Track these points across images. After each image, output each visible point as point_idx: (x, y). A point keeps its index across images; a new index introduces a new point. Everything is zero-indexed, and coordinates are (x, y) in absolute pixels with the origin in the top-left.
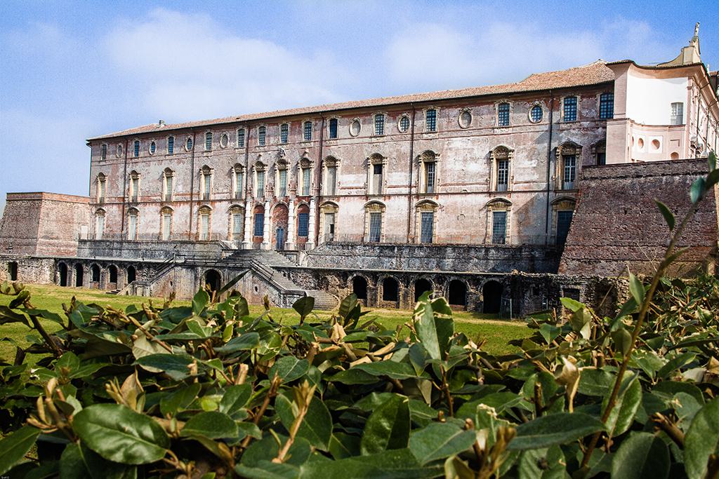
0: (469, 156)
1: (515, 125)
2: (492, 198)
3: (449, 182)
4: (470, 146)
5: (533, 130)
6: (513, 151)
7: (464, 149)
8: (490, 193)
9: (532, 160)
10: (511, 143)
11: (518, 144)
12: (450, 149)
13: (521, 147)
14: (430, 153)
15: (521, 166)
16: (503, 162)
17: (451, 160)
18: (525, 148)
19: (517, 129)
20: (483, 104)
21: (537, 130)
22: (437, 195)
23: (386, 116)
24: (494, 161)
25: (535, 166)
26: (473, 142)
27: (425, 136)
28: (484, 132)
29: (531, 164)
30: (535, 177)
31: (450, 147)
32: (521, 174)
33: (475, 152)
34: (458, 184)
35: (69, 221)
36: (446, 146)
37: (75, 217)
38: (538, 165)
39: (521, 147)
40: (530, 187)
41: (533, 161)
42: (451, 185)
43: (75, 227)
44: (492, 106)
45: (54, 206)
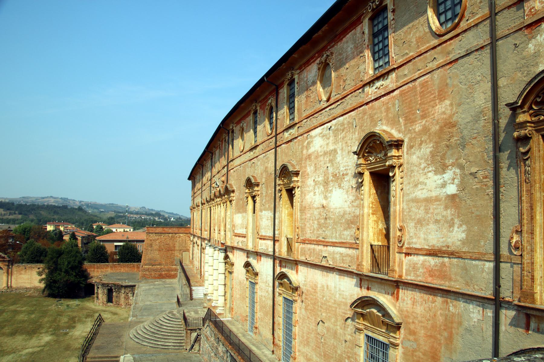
0: (331, 170)
1: (400, 61)
2: (364, 293)
3: (309, 235)
4: (331, 147)
5: (441, 60)
6: (398, 144)
7: (325, 153)
8: (363, 279)
9: (443, 168)
10: (394, 122)
11: (410, 120)
12: (309, 157)
13: (418, 127)
14: (285, 172)
15: (421, 194)
16: (382, 180)
17: (310, 182)
18: (425, 130)
19: (405, 70)
20: (346, 32)
21: (452, 57)
22: (296, 263)
23: (258, 108)
24: (367, 176)
25: (452, 189)
26: (336, 132)
27: (286, 134)
28: (351, 102)
29: (444, 185)
30: (457, 236)
31: (311, 150)
32: (420, 222)
33: (339, 158)
34: (318, 243)
35: (170, 249)
36: (305, 152)
37: (177, 245)
38: (462, 187)
39: (418, 127)
40: (442, 274)
41: (448, 175)
42: (310, 242)
43: (177, 253)
44: (359, 29)
45: (157, 237)
